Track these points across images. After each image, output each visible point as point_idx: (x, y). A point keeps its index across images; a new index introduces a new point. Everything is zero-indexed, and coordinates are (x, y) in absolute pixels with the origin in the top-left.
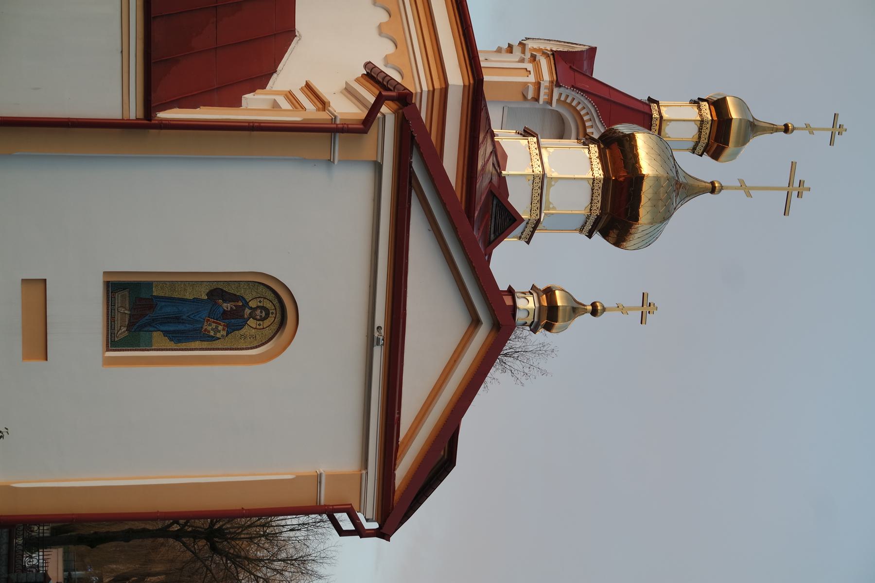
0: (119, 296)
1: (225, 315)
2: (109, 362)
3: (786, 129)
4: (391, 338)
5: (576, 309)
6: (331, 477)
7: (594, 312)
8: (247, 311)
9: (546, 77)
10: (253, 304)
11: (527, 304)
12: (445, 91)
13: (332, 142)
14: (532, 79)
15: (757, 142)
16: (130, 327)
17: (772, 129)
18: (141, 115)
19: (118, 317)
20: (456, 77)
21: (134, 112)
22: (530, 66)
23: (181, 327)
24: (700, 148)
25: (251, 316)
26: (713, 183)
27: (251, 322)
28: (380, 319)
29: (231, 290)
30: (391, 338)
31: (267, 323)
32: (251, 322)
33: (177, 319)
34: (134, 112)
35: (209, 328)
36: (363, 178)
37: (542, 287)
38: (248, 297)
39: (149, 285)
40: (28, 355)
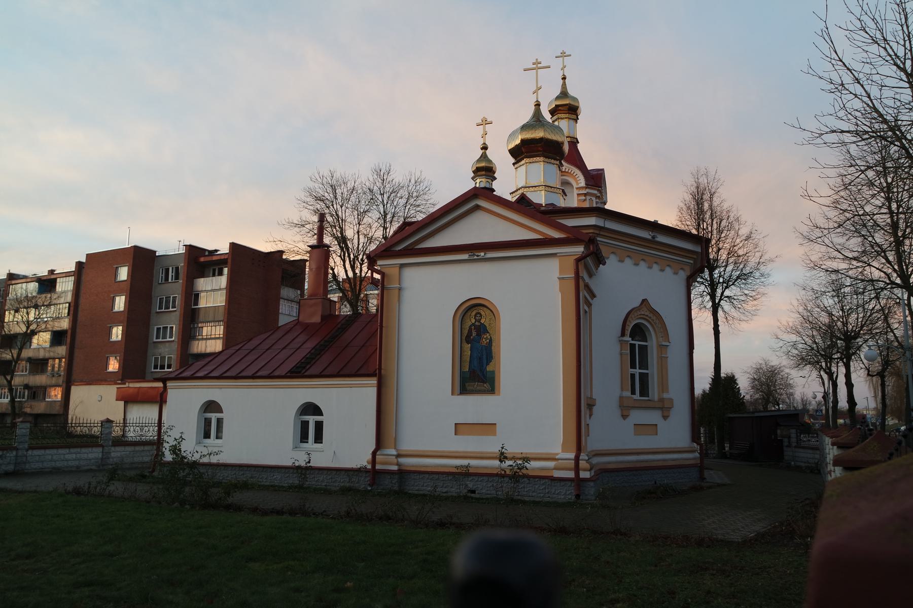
0: (469, 388)
1: (479, 335)
2: (499, 394)
3: (564, 78)
4: (476, 251)
5: (484, 157)
6: (561, 272)
8: (477, 323)
10: (473, 321)
13: (389, 289)
15: (571, 91)
16: (484, 382)
18: (375, 378)
19: (478, 388)
21: (374, 381)
23: (485, 357)
24: (574, 117)
25: (479, 321)
27: (482, 321)
29: (466, 332)
30: (476, 251)
31: (483, 313)
32: (482, 321)
33: (480, 359)
34: (374, 381)
35: (485, 342)
36: (408, 273)
38: (470, 323)
39: (462, 373)
40: (494, 434)
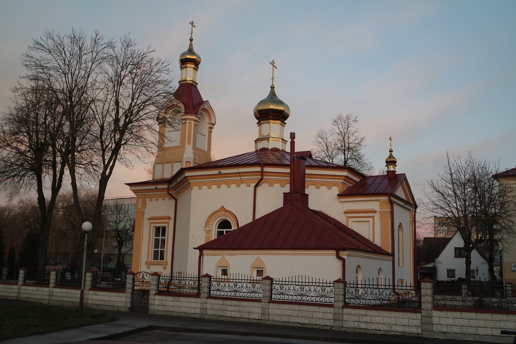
3: (191, 40)
7: (392, 151)
9: (193, 117)
11: (391, 168)
12: (346, 177)
14: (193, 122)
17: (191, 45)
20: (345, 173)
22: (188, 121)
26: (271, 88)
28: (403, 204)
37: (386, 164)
